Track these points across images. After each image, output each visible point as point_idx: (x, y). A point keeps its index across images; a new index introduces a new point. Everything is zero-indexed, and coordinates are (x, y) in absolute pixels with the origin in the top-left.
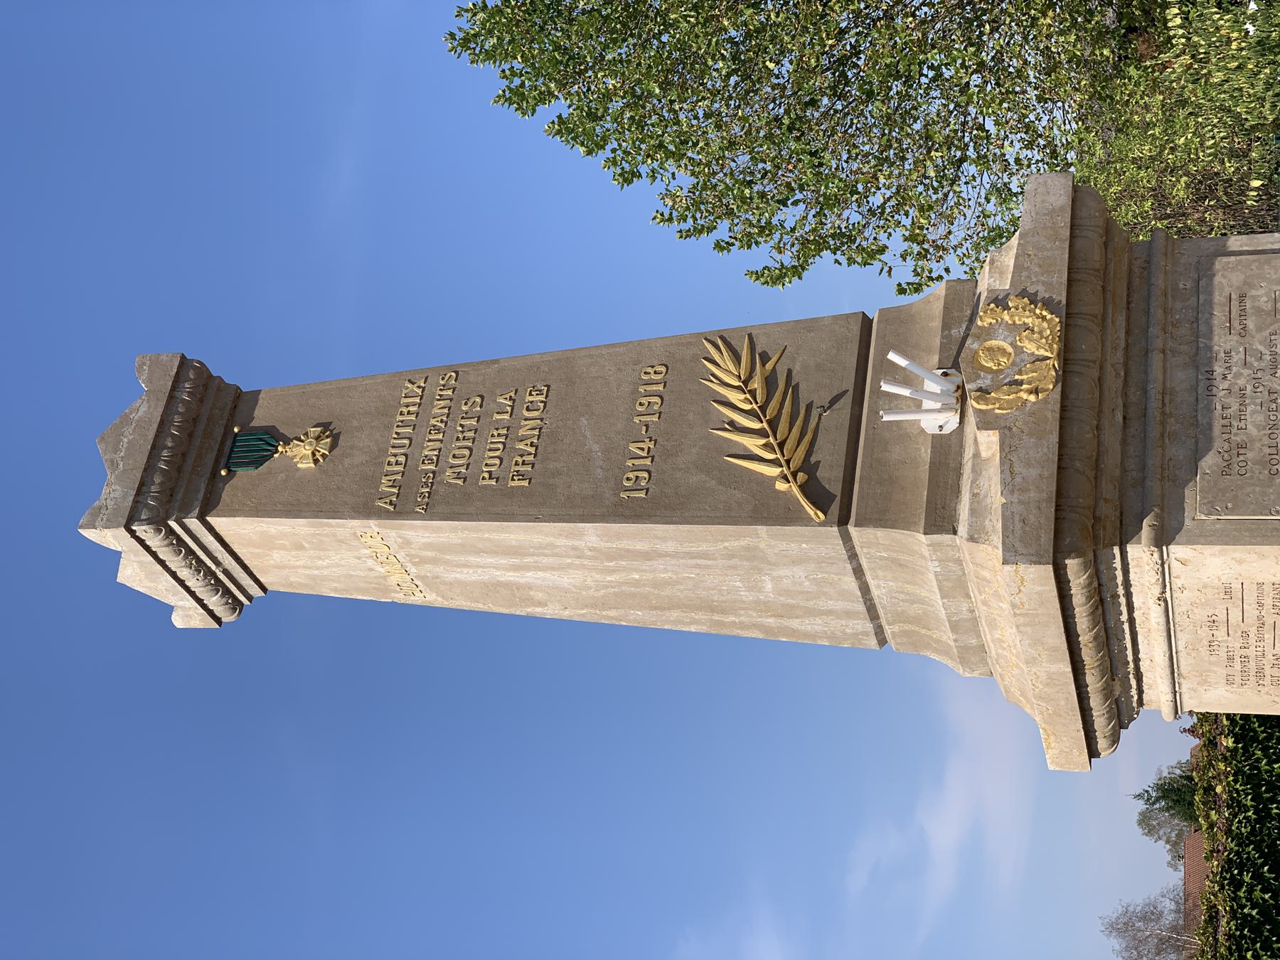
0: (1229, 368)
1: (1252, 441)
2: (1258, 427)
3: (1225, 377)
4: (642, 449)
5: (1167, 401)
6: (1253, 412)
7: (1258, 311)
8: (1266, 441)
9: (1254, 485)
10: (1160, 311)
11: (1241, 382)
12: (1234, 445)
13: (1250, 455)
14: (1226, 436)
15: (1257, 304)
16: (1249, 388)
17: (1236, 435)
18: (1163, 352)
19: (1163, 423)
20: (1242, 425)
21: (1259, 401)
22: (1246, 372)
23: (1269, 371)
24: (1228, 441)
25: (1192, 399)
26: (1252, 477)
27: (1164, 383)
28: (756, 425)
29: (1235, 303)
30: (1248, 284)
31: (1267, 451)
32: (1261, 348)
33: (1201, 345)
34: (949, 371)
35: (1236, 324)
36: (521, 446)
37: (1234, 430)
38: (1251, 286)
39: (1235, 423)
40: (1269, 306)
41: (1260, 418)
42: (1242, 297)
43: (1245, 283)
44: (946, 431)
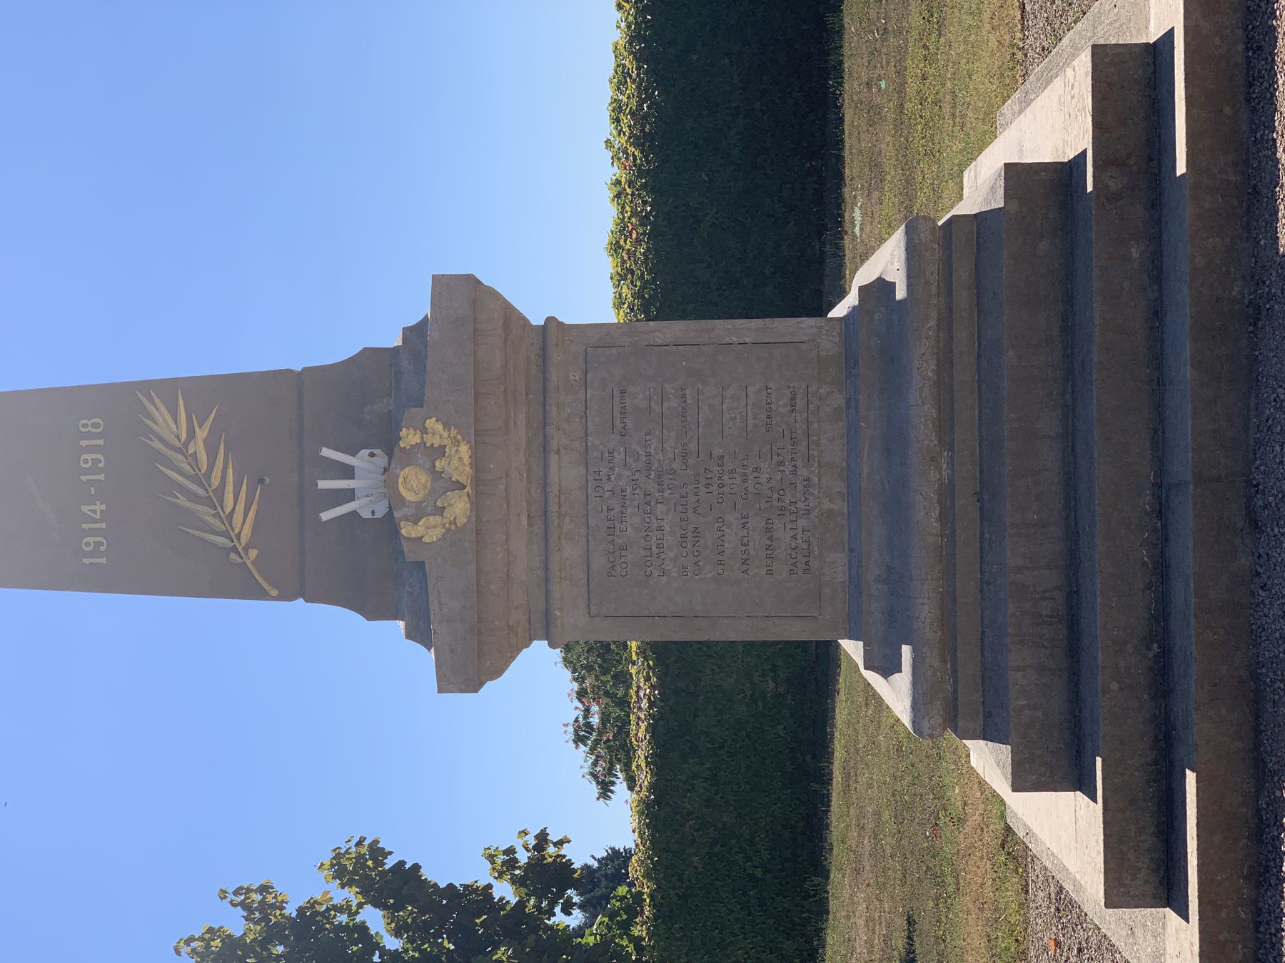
0: (612, 469)
4: (94, 512)
13: (630, 557)
16: (629, 489)
18: (558, 452)
20: (623, 527)
21: (636, 503)
22: (627, 473)
24: (612, 542)
28: (200, 491)
29: (617, 399)
31: (643, 553)
34: (375, 451)
37: (617, 532)
42: (623, 392)
44: (379, 515)
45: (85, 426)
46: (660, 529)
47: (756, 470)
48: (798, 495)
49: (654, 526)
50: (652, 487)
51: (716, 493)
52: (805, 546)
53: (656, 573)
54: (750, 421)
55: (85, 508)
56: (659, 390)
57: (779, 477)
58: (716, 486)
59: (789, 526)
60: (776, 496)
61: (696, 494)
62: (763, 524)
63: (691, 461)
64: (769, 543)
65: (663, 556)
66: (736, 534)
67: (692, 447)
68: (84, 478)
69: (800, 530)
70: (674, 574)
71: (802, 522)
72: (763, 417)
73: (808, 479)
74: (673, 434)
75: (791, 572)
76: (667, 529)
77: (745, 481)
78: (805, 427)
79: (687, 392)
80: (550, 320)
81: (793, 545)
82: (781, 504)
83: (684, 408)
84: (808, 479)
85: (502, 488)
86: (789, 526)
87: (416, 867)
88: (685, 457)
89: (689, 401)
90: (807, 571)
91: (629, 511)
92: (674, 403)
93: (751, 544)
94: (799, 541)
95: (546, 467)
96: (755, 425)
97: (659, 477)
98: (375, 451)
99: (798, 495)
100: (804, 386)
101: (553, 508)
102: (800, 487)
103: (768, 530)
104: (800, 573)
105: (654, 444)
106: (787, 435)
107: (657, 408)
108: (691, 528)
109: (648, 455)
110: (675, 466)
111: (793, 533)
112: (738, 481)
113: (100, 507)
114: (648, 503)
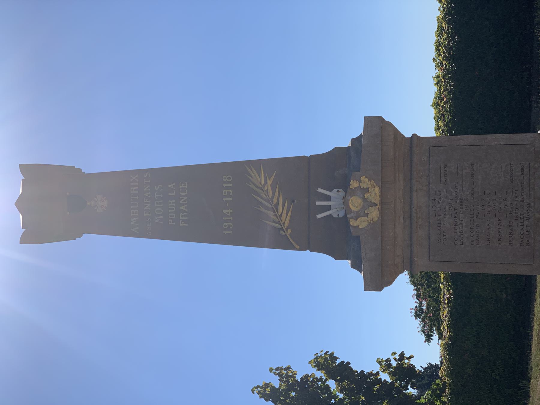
4: (228, 213)
10: (415, 173)
13: (447, 236)
14: (439, 228)
16: (447, 207)
21: (451, 213)
36: (181, 208)
37: (442, 225)
39: (442, 223)
42: (445, 166)
44: (341, 216)
45: (225, 178)
46: (461, 224)
47: (505, 200)
52: (527, 233)
53: (459, 243)
55: (224, 212)
57: (515, 203)
58: (486, 207)
59: (520, 224)
65: (462, 236)
68: (224, 199)
69: (525, 226)
70: (467, 244)
73: (529, 204)
75: (521, 245)
76: (464, 224)
80: (414, 135)
82: (516, 215)
83: (472, 173)
84: (529, 204)
85: (393, 206)
86: (520, 224)
87: (348, 363)
89: (475, 170)
90: (528, 244)
93: (502, 232)
95: (411, 198)
98: (339, 190)
102: (525, 208)
103: (510, 226)
109: (456, 192)
110: (468, 198)
111: (522, 227)
113: (230, 211)
114: (456, 213)
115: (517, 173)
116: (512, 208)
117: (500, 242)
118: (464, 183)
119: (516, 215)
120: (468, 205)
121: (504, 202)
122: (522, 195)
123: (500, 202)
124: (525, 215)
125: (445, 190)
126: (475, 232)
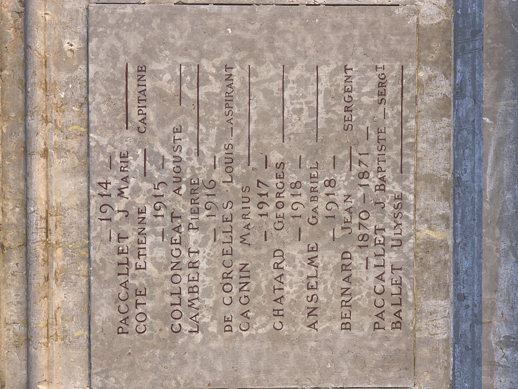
0: (125, 179)
1: (152, 285)
2: (159, 266)
3: (121, 194)
5: (52, 226)
6: (155, 245)
7: (161, 94)
8: (168, 286)
9: (154, 347)
11: (140, 200)
12: (132, 292)
13: (149, 305)
14: (122, 279)
15: (158, 84)
16: (149, 210)
17: (134, 277)
18: (45, 154)
19: (46, 262)
20: (141, 263)
21: (159, 229)
22: (146, 186)
23: (172, 186)
24: (125, 285)
25: (83, 221)
26: (151, 336)
27: (47, 202)
29: (132, 81)
30: (149, 50)
31: (169, 299)
32: (163, 151)
33: (93, 144)
35: (134, 112)
37: (132, 271)
38: (153, 55)
39: (133, 261)
40: (171, 89)
41: (160, 253)
42: (142, 70)
43: (144, 50)
46: (193, 265)
47: (330, 183)
48: (387, 220)
49: (185, 261)
50: (183, 206)
51: (273, 216)
52: (395, 290)
53: (186, 327)
54: (322, 115)
56: (194, 69)
57: (360, 194)
58: (272, 206)
59: (373, 261)
60: (356, 221)
61: (244, 217)
62: (338, 260)
63: (238, 170)
64: (345, 285)
65: (197, 304)
66: (301, 273)
67: (240, 150)
69: (388, 268)
70: (213, 329)
71: (391, 257)
72: (340, 109)
73: (400, 197)
74: (214, 131)
75: (376, 327)
76: (203, 265)
77: (313, 199)
78: (397, 124)
79: (234, 71)
81: (379, 288)
82: (363, 231)
84: (400, 197)
86: (373, 261)
88: (229, 164)
89: (237, 84)
90: (398, 325)
91: (150, 239)
92: (215, 87)
93: (321, 287)
94: (387, 283)
95: (27, 176)
96: (329, 121)
97: (193, 192)
99: (387, 220)
100: (397, 66)
101: (38, 236)
102: (389, 209)
103: (345, 268)
104: (388, 328)
105: (187, 144)
106: (373, 136)
107: (191, 94)
108: (237, 264)
109: (178, 160)
110: (215, 177)
111: (379, 271)
112: (304, 198)
114: (177, 229)
115: (365, 100)
116: (348, 210)
117: (312, 319)
118: (201, 127)
119: (363, 231)
120: (215, 200)
121: (329, 190)
122: (380, 170)
123: (313, 190)
124: (389, 233)
125: (140, 152)
126: (235, 290)
